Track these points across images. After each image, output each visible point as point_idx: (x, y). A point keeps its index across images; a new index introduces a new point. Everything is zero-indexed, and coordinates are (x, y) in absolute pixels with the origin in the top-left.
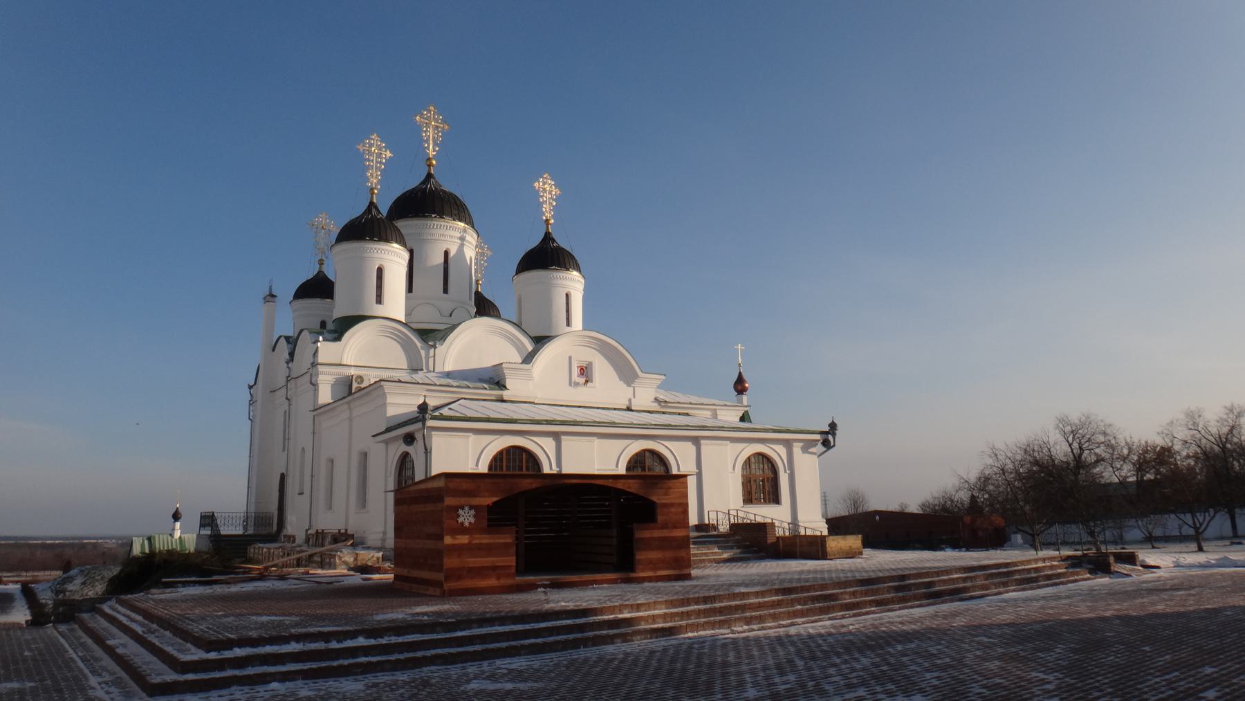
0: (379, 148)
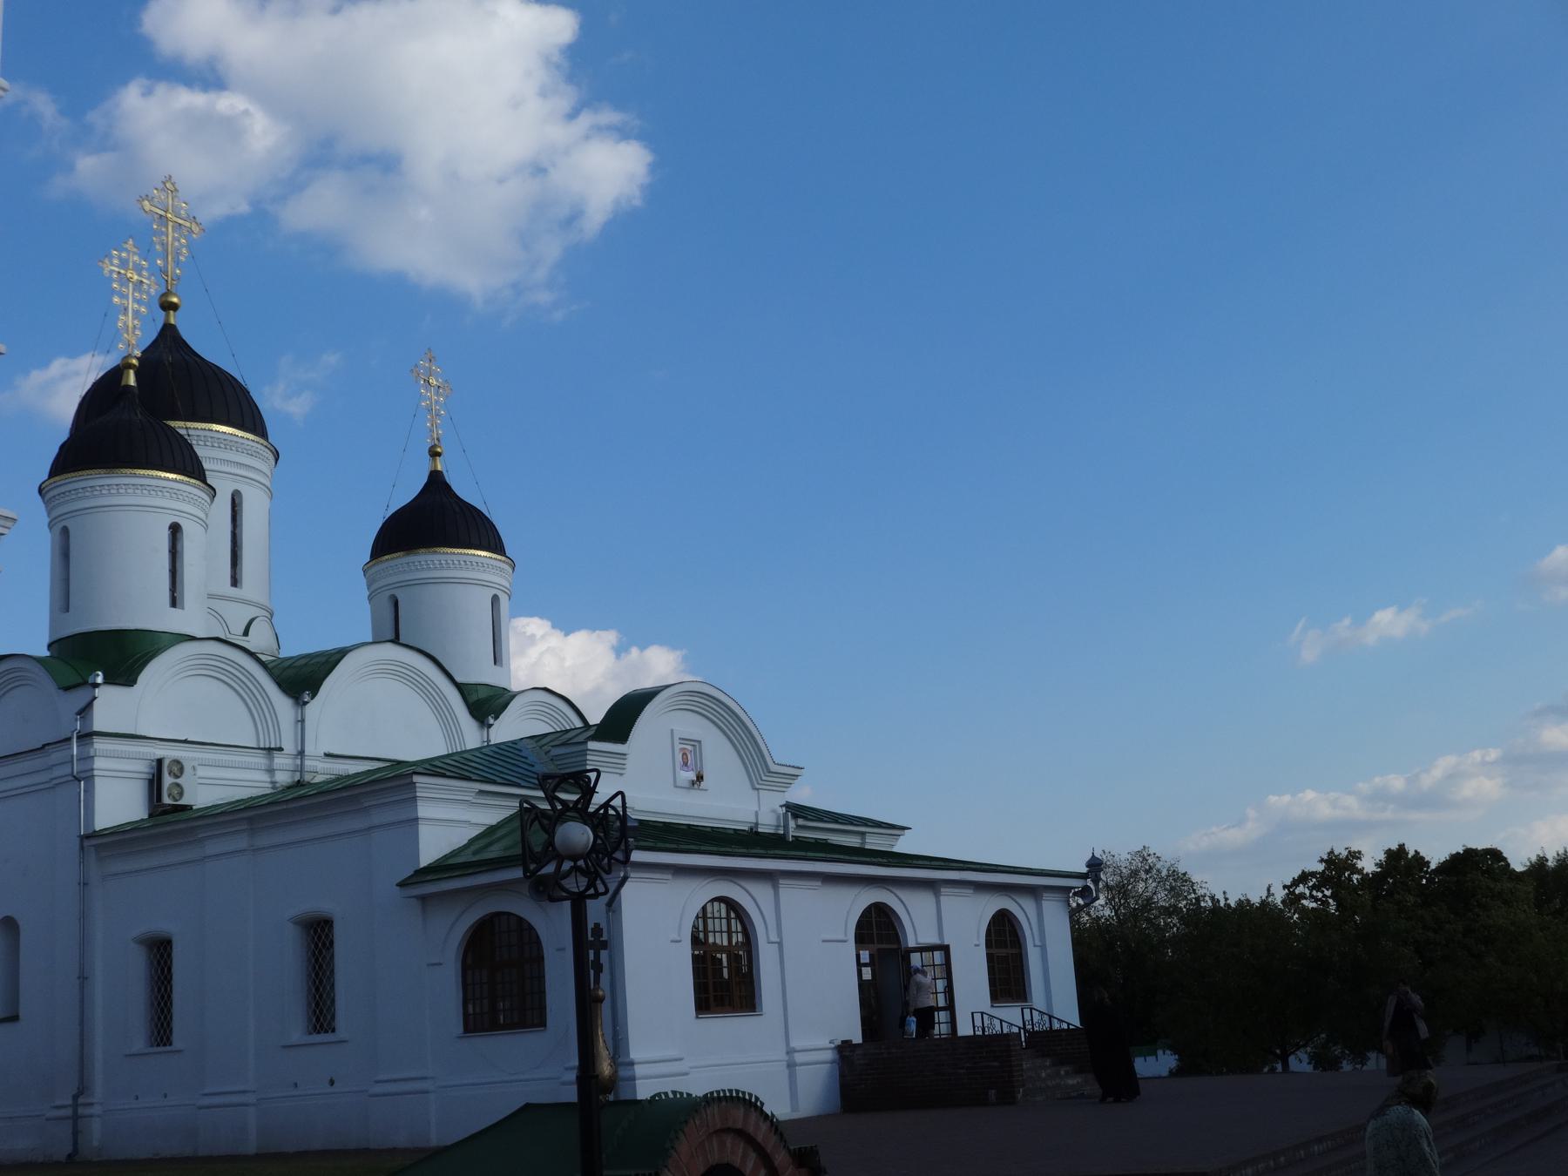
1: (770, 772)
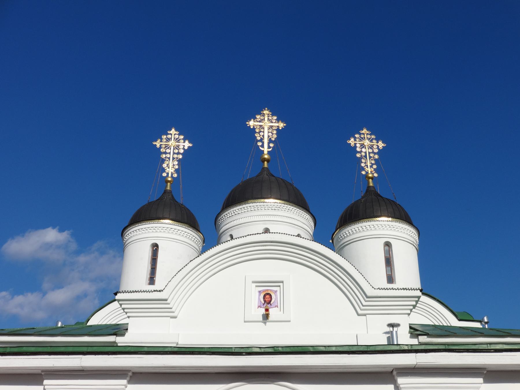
0: (177, 140)
1: (367, 297)
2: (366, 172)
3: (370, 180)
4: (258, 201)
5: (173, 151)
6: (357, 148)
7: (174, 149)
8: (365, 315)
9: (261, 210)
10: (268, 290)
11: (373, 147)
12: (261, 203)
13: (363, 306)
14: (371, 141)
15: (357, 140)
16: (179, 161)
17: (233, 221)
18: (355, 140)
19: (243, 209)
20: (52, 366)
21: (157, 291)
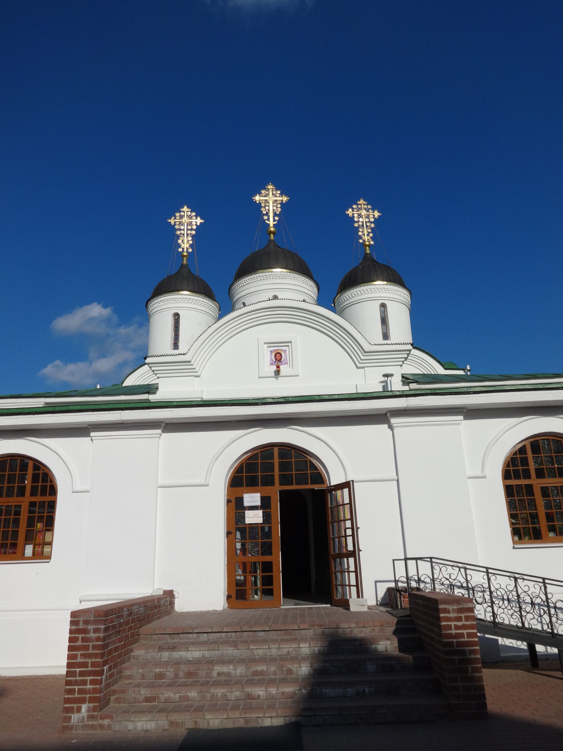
0: (190, 217)
1: (365, 352)
2: (363, 240)
3: (367, 248)
4: (267, 271)
5: (187, 227)
6: (355, 218)
7: (187, 225)
8: (363, 368)
9: (270, 279)
10: (278, 350)
11: (369, 217)
12: (269, 273)
13: (362, 360)
14: (368, 211)
15: (355, 210)
16: (193, 236)
17: (245, 290)
18: (353, 211)
19: (253, 279)
20: (96, 420)
21: (181, 354)
